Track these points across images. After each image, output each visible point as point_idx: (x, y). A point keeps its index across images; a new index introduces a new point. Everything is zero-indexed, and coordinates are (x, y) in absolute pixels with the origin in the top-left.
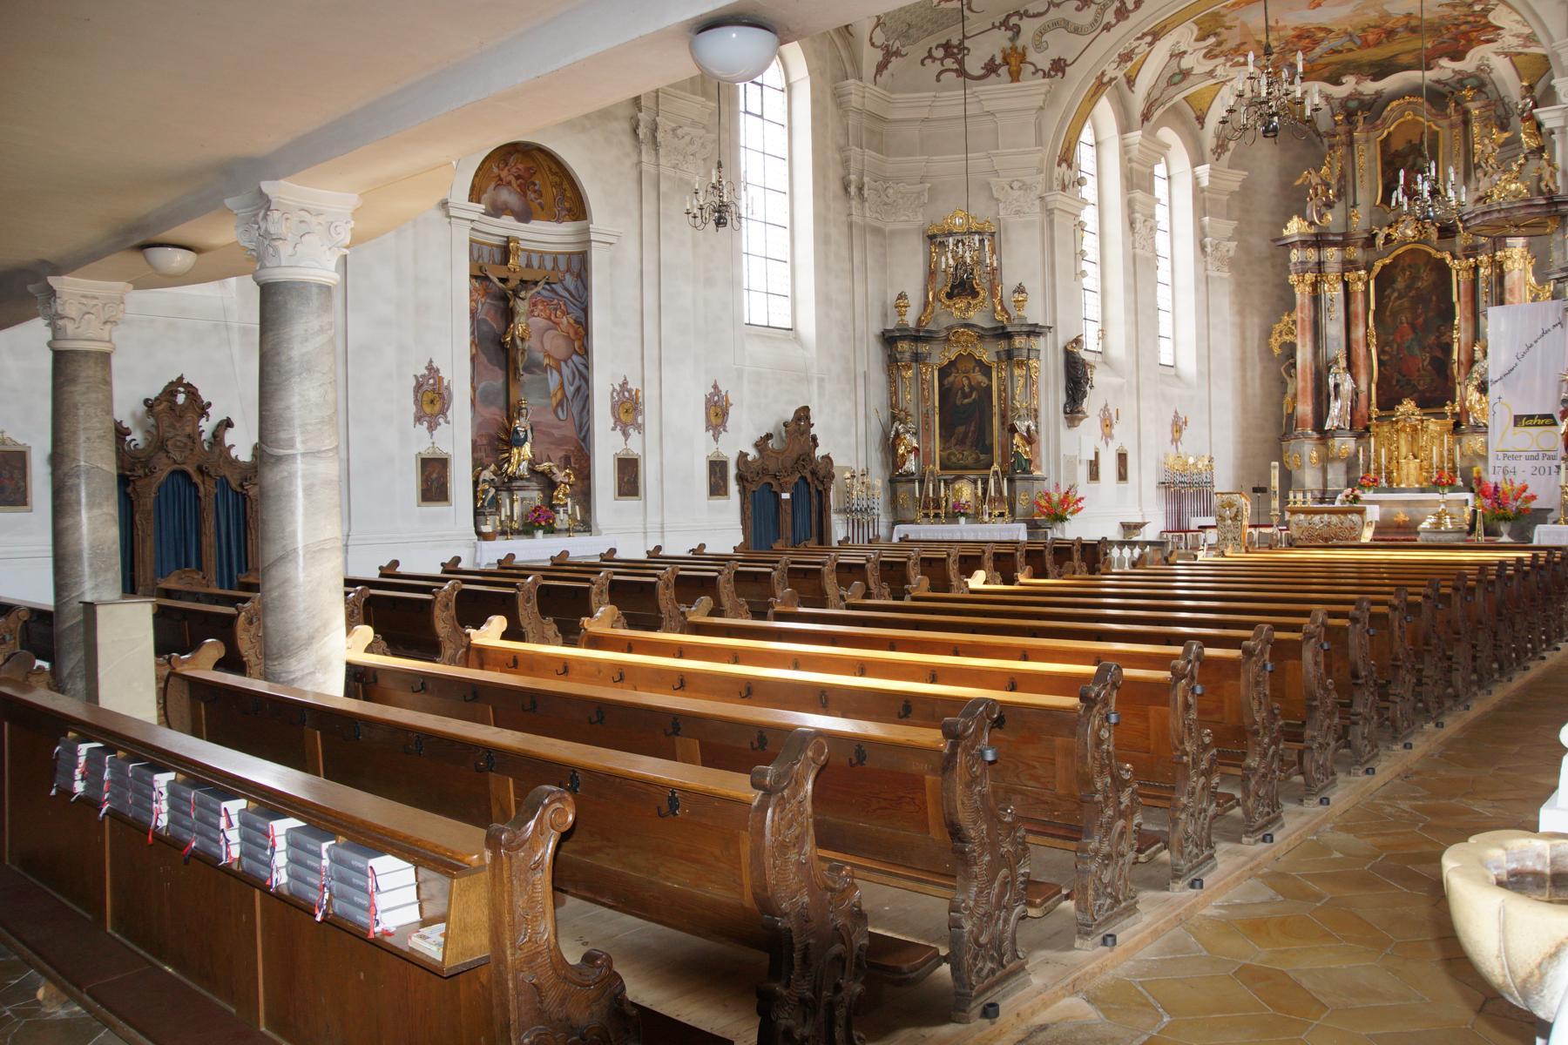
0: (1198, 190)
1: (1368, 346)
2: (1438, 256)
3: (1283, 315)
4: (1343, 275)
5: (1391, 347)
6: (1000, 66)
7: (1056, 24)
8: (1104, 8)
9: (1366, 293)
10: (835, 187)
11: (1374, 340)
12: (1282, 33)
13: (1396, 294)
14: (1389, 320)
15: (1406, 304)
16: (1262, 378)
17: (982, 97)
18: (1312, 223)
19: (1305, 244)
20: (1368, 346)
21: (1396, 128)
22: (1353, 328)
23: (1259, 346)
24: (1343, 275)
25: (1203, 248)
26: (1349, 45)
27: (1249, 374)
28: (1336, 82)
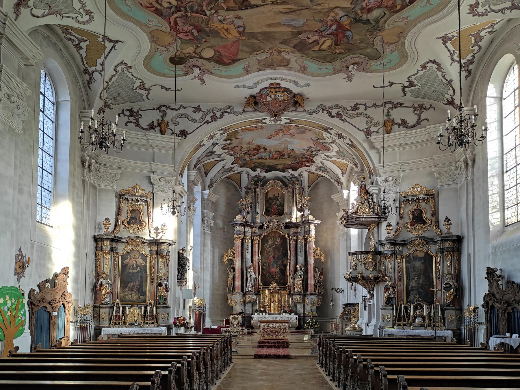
0: (203, 199)
1: (259, 263)
2: (283, 234)
4: (252, 237)
5: (266, 264)
6: (155, 127)
7: (183, 116)
8: (206, 114)
9: (259, 244)
10: (78, 161)
12: (251, 146)
13: (268, 246)
14: (266, 254)
15: (272, 250)
16: (219, 271)
17: (149, 138)
18: (244, 218)
19: (241, 225)
20: (259, 263)
22: (254, 256)
24: (252, 237)
25: (203, 221)
26: (267, 157)
27: (215, 270)
28: (254, 170)
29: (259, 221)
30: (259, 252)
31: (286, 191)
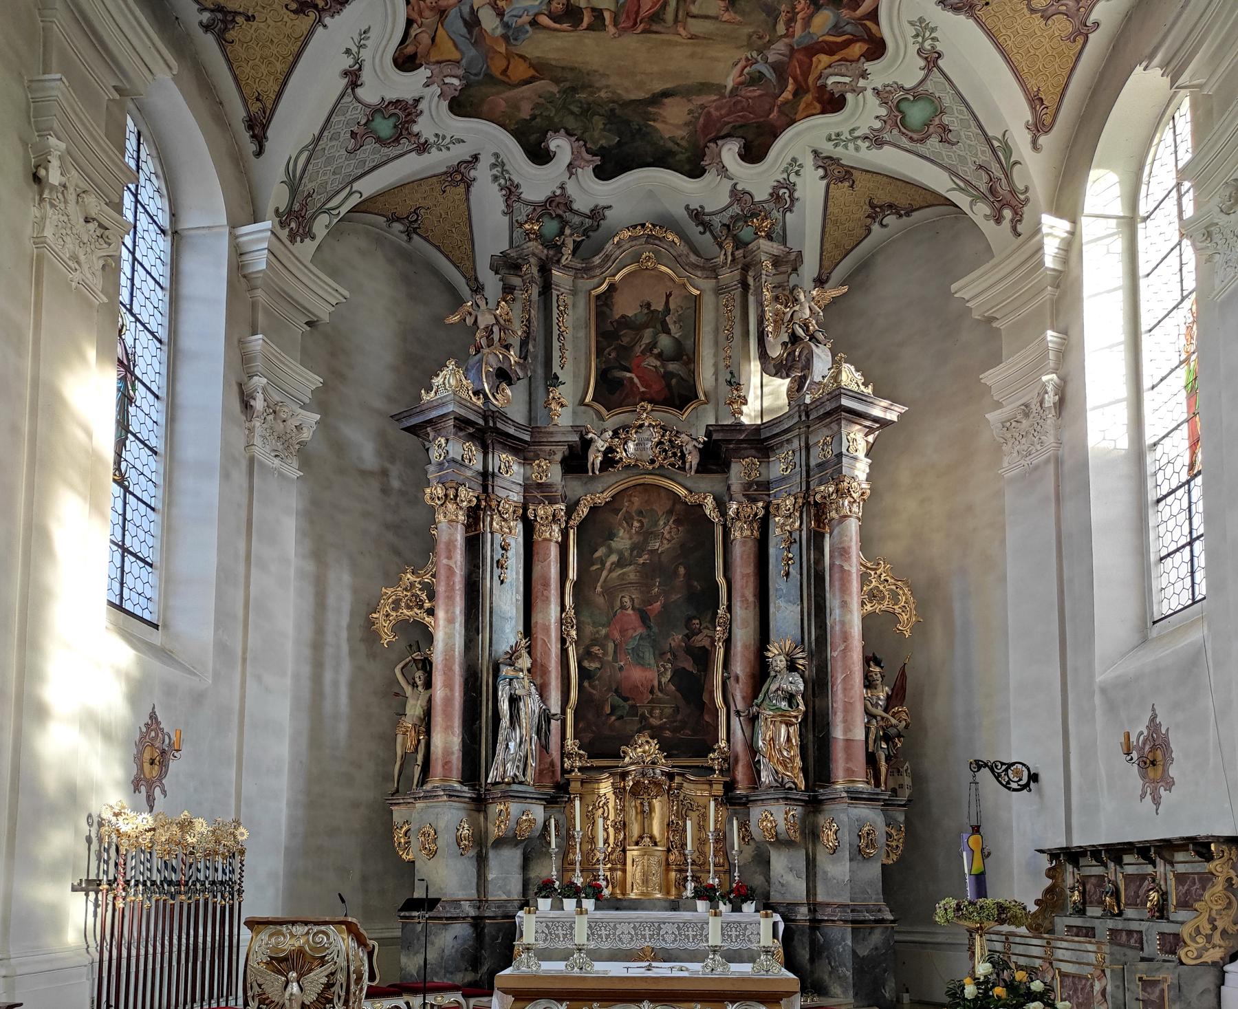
3: (405, 573)
5: (603, 647)
11: (574, 633)
20: (563, 641)
21: (624, 278)
22: (538, 605)
23: (350, 627)
28: (540, 156)
29: (564, 418)
30: (569, 587)
31: (708, 284)
